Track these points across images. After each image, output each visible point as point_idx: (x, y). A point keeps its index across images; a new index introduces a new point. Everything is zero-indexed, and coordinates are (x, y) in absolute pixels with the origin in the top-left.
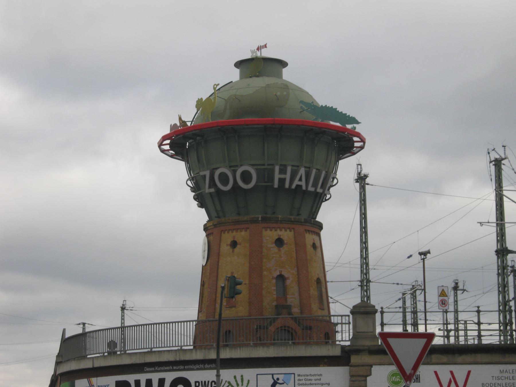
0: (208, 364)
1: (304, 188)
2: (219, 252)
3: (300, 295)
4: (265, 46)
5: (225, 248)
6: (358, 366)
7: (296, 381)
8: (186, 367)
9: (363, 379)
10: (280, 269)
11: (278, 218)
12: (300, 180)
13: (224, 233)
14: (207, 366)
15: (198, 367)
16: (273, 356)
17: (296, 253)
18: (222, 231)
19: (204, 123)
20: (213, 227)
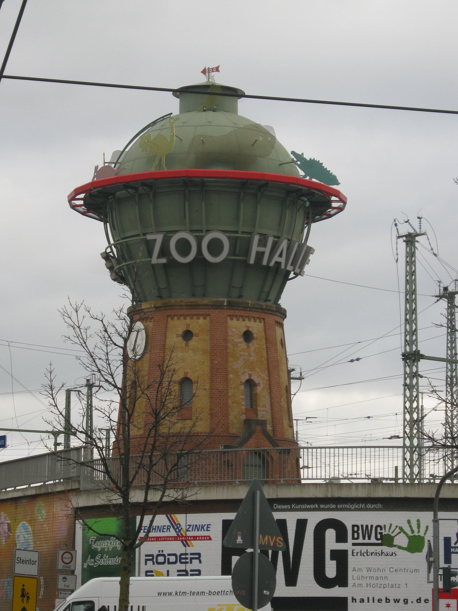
0: (371, 504)
1: (283, 266)
4: (217, 69)
5: (174, 339)
10: (250, 372)
11: (247, 304)
12: (281, 256)
13: (172, 319)
14: (369, 506)
17: (267, 351)
18: (168, 316)
19: (153, 169)
20: (154, 309)
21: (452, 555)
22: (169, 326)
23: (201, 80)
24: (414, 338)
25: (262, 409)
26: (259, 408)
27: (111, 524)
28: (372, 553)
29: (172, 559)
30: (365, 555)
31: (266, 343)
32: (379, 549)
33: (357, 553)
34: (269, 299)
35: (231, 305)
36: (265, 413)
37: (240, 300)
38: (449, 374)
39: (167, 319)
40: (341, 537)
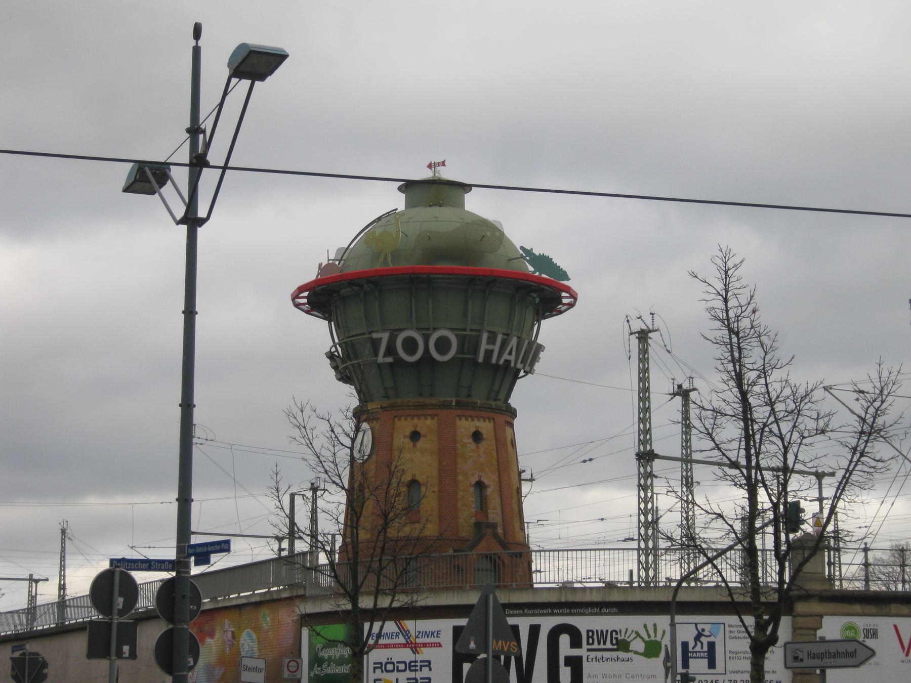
1: (512, 365)
2: (392, 447)
4: (443, 164)
9: (813, 632)
11: (476, 403)
12: (510, 353)
13: (399, 419)
14: (604, 610)
15: (591, 611)
17: (497, 452)
19: (378, 266)
23: (427, 174)
24: (648, 437)
27: (338, 631)
29: (402, 667)
32: (614, 654)
35: (460, 405)
37: (469, 400)
38: (684, 474)
40: (576, 642)
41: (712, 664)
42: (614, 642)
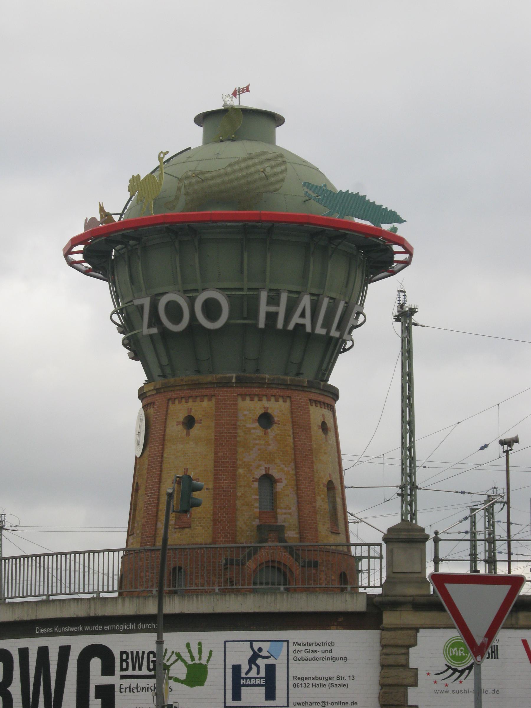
0: (143, 623)
1: (308, 329)
2: (164, 435)
3: (299, 509)
4: (247, 89)
5: (175, 429)
6: (395, 629)
7: (291, 653)
8: (106, 628)
9: (403, 651)
10: (267, 466)
12: (303, 315)
13: (173, 403)
14: (141, 626)
16: (252, 611)
17: (294, 438)
18: (169, 400)
19: (143, 216)
20: (155, 392)
21: (243, 688)
22: (169, 411)
25: (284, 511)
26: (278, 510)
28: (143, 689)
30: (135, 690)
31: (293, 428)
33: (126, 688)
34: (301, 372)
35: (240, 381)
36: (289, 516)
39: (168, 403)
41: (270, 695)
42: (151, 667)
